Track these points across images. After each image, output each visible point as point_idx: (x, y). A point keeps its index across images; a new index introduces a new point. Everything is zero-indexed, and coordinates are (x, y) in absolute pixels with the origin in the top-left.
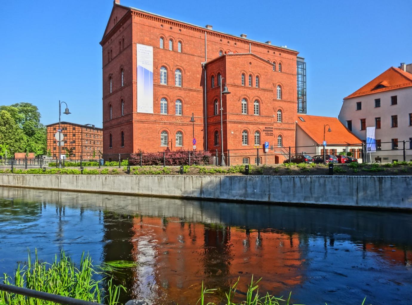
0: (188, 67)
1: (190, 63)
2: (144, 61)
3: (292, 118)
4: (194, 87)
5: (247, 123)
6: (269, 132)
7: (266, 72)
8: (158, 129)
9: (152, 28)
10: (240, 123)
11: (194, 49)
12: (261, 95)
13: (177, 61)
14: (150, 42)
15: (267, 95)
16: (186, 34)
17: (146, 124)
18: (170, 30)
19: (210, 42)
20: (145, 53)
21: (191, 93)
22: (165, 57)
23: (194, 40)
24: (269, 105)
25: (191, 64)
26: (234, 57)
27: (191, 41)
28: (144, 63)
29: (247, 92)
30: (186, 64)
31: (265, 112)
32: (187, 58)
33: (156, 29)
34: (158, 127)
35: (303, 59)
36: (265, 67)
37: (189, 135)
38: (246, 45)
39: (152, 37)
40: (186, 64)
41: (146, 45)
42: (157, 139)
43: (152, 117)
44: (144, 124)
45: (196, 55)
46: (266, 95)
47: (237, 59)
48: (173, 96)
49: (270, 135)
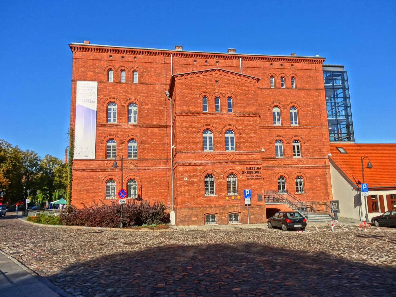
0: (146, 99)
1: (149, 94)
2: (85, 99)
3: (320, 150)
4: (155, 123)
5: (212, 164)
6: (254, 175)
7: (245, 90)
8: (102, 177)
9: (97, 61)
10: (200, 164)
11: (155, 77)
12: (238, 122)
13: (131, 94)
14: (94, 77)
15: (249, 121)
16: (144, 61)
17: (86, 173)
18: (121, 59)
19: (178, 65)
20: (86, 90)
21: (150, 130)
22: (114, 91)
23: (155, 66)
24: (252, 135)
25: (150, 95)
26: (189, 76)
27: (151, 68)
28: (85, 101)
29: (211, 120)
30: (143, 96)
31: (246, 146)
32: (144, 88)
33: (102, 62)
34: (102, 175)
35: (343, 67)
36: (243, 84)
37: (146, 184)
38: (234, 62)
39: (97, 71)
40: (143, 96)
41: (89, 81)
42: (100, 190)
43: (94, 164)
44: (83, 173)
45: (157, 83)
46: (246, 122)
47: (194, 79)
48: (123, 136)
49: (256, 179)
